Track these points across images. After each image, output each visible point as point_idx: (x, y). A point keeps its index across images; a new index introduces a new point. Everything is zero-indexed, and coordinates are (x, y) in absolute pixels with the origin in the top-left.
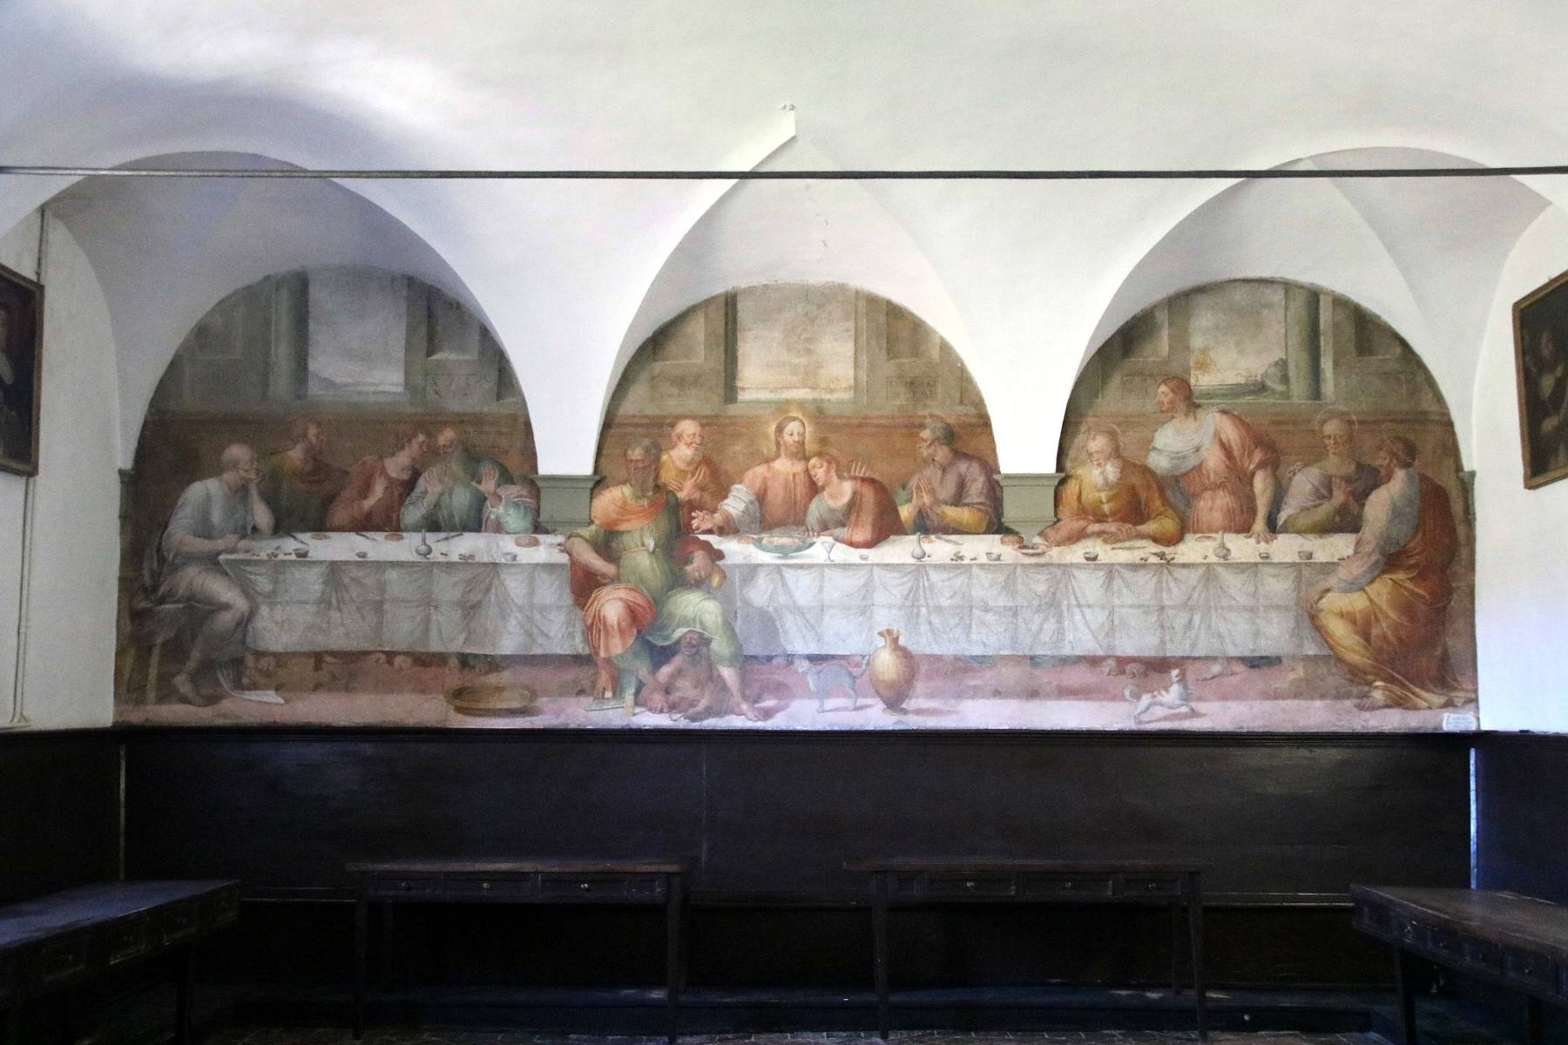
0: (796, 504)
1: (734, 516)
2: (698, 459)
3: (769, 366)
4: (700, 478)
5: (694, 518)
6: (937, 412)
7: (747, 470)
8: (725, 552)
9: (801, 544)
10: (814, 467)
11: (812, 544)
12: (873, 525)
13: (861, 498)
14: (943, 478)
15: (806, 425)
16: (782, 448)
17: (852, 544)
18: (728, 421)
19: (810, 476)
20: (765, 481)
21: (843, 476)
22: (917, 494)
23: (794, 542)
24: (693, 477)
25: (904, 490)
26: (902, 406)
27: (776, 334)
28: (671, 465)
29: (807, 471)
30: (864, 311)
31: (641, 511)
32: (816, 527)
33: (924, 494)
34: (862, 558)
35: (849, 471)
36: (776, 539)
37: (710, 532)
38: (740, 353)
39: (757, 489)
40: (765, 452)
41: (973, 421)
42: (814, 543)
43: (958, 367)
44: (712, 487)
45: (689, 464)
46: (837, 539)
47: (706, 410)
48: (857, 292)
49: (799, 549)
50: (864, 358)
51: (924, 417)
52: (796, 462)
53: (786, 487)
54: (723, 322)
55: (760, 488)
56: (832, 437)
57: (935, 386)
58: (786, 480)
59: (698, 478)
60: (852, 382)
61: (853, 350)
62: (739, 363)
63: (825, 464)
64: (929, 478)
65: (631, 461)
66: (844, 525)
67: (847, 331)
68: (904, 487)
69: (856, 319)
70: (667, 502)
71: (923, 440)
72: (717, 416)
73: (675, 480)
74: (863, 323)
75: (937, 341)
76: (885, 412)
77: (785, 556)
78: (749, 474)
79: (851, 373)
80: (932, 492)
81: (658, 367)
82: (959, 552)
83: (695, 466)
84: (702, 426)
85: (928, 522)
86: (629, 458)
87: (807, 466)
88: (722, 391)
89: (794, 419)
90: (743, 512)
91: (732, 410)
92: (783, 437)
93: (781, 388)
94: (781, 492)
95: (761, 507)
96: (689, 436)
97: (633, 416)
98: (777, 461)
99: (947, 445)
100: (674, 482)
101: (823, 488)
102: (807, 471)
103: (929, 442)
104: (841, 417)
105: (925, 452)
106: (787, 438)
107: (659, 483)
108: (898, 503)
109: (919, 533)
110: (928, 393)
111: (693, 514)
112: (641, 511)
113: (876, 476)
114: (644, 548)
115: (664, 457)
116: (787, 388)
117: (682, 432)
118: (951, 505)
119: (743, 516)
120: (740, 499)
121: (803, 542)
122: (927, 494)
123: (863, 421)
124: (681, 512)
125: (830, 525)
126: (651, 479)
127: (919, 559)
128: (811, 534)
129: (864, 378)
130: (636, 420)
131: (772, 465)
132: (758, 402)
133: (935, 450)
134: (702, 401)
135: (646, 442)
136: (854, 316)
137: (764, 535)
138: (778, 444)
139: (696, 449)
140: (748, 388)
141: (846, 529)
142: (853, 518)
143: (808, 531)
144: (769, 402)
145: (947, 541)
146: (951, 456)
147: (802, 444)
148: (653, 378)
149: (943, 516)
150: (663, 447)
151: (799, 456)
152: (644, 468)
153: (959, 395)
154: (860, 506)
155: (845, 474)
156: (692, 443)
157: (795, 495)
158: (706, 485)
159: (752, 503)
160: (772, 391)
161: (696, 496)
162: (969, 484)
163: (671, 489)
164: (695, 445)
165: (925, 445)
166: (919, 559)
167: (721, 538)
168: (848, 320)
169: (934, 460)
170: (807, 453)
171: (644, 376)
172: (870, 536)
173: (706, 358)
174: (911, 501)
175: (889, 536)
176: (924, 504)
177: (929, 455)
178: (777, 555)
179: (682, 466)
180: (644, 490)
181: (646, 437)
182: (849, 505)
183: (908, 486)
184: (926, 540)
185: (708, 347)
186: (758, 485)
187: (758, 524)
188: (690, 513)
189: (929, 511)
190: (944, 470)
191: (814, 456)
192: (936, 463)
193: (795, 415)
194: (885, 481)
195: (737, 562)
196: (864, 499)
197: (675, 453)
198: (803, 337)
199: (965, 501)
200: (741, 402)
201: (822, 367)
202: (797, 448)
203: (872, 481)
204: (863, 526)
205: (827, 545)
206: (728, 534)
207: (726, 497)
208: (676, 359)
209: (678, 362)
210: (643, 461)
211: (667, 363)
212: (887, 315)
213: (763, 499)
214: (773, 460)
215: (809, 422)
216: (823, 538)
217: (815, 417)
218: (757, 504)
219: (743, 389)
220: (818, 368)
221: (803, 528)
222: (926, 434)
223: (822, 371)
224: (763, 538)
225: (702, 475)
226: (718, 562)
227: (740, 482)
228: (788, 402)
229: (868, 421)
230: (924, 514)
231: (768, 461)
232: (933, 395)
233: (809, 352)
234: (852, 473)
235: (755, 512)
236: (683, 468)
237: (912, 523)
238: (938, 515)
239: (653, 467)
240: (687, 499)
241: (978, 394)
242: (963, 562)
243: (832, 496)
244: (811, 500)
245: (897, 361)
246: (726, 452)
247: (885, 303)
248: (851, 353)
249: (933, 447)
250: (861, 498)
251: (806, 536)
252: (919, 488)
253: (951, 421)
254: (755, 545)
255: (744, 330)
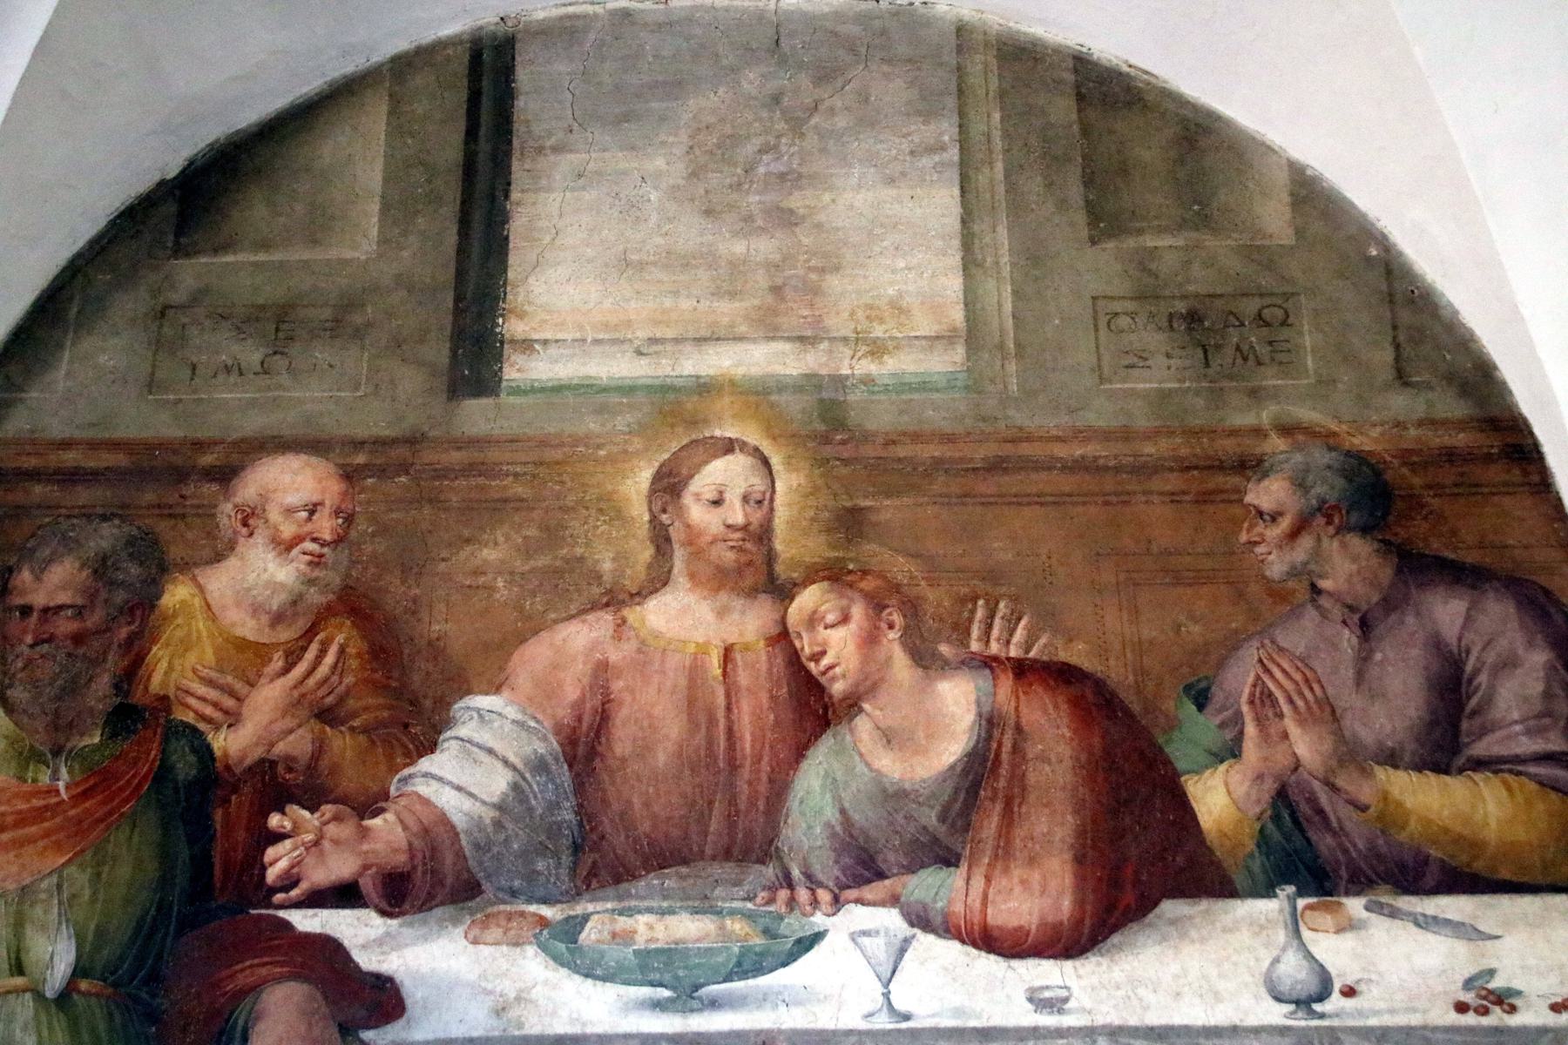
0: (733, 766)
1: (459, 820)
2: (316, 598)
3: (627, 265)
4: (324, 670)
5: (278, 837)
6: (1307, 414)
7: (522, 639)
8: (413, 993)
9: (758, 941)
10: (813, 620)
11: (807, 943)
12: (1079, 860)
13: (1016, 749)
14: (1363, 660)
15: (776, 461)
16: (679, 557)
17: (990, 940)
18: (456, 457)
19: (794, 661)
20: (602, 669)
21: (935, 655)
22: (1260, 721)
23: (724, 933)
24: (286, 670)
25: (1201, 707)
26: (1164, 396)
27: (660, 163)
28: (201, 625)
29: (782, 637)
30: (994, 83)
31: (38, 815)
32: (826, 867)
33: (1294, 731)
34: (1040, 1000)
35: (961, 632)
36: (642, 920)
37: (344, 895)
38: (517, 227)
39: (564, 714)
40: (607, 566)
41: (1461, 439)
42: (817, 937)
43: (1369, 260)
44: (369, 709)
45: (278, 619)
46: (921, 920)
47: (375, 421)
48: (962, 30)
49: (752, 964)
50: (1000, 239)
51: (1258, 432)
52: (738, 603)
53: (691, 702)
54: (462, 125)
55: (578, 705)
56: (888, 511)
57: (1284, 323)
58: (695, 672)
59: (310, 672)
60: (957, 315)
61: (956, 210)
62: (513, 259)
63: (858, 611)
64: (1304, 661)
65: (26, 610)
66: (949, 860)
67: (931, 150)
68: (1201, 700)
69: (962, 114)
70: (163, 773)
71: (1260, 514)
72: (413, 441)
73: (210, 683)
74: (990, 121)
75: (1282, 177)
76: (1100, 415)
77: (687, 996)
78: (534, 656)
79: (953, 285)
80: (1327, 713)
81: (189, 274)
82: (1491, 973)
83: (302, 624)
84: (350, 475)
85: (1325, 843)
86: (19, 601)
87: (783, 621)
88: (438, 351)
89: (729, 447)
90: (500, 807)
91: (475, 416)
92: (681, 511)
93: (676, 341)
94: (673, 728)
95: (579, 787)
96: (290, 511)
97: (66, 444)
98: (652, 604)
99: (1365, 530)
100: (202, 690)
101: (853, 704)
102: (782, 637)
103: (1285, 523)
104: (916, 437)
105: (1276, 567)
106: (697, 513)
107: (138, 698)
108: (1180, 765)
109: (1291, 889)
110: (1263, 351)
111: (275, 820)
112: (38, 815)
113: (1077, 654)
114: (19, 981)
115: (177, 594)
116: (700, 341)
117: (264, 497)
118: (1419, 768)
119: (498, 824)
120: (490, 751)
121: (767, 932)
122: (1301, 722)
123: (1008, 449)
124: (218, 815)
125: (890, 858)
126: (102, 685)
127: (1304, 1003)
128: (803, 894)
129: (1000, 297)
130: (70, 458)
131: (632, 614)
132: (585, 389)
133: (1317, 553)
134: (357, 389)
135: (105, 537)
136: (951, 102)
137: (590, 907)
138: (661, 540)
139: (317, 561)
140: (545, 342)
141: (956, 877)
142: (989, 825)
143: (790, 884)
144: (628, 389)
145: (1427, 923)
146: (1386, 574)
147: (762, 535)
148: (162, 313)
149: (1389, 817)
150: (175, 552)
151: (749, 581)
152: (78, 639)
153: (1388, 355)
154: (1018, 776)
155: (944, 649)
156: (298, 540)
157: (730, 732)
158: (341, 700)
159: (540, 766)
160: (639, 353)
161: (297, 744)
162: (1483, 678)
163: (190, 718)
164: (309, 546)
165: (1275, 532)
166: (1304, 1003)
167: (394, 923)
168: (928, 115)
169: (1315, 590)
170: (779, 568)
171: (129, 304)
172: (1067, 904)
173: (383, 241)
174: (1233, 751)
175: (1156, 904)
176: (1297, 766)
177: (1294, 572)
178: (645, 992)
179: (248, 628)
180: (61, 727)
181: (104, 518)
182: (965, 772)
183: (1218, 696)
184: (1327, 920)
185: (397, 209)
186: (572, 693)
187: (566, 859)
188: (266, 816)
189: (1316, 785)
190: (1365, 627)
191: (808, 581)
192: (1324, 602)
193: (731, 433)
194: (1117, 673)
195: (457, 1031)
196: (1033, 749)
197: (220, 581)
198: (762, 170)
199: (1480, 749)
200: (517, 391)
201: (837, 269)
202: (741, 550)
203: (1061, 675)
204: (1032, 861)
205: (877, 946)
206: (426, 905)
207: (430, 747)
208: (265, 245)
209: (277, 256)
210: (79, 611)
211: (230, 258)
212: (1080, 98)
213: (592, 753)
214: (640, 595)
215: (788, 460)
216: (857, 916)
217: (814, 436)
218: (565, 776)
219: (527, 345)
220: (822, 271)
221: (770, 872)
222: (1269, 493)
223: (834, 282)
224: (586, 918)
225: (330, 659)
226: (367, 1035)
227: (497, 690)
228: (705, 388)
229: (1026, 449)
230: (1304, 808)
231: (616, 599)
232: (1282, 355)
233: (786, 219)
234: (975, 646)
235: (553, 806)
236: (251, 636)
237: (1251, 845)
238: (1363, 808)
239: (124, 632)
240: (258, 753)
241: (1464, 342)
242: (1515, 1021)
243: (889, 737)
244: (800, 752)
245: (1131, 243)
246: (442, 566)
247: (1070, 63)
248: (953, 221)
249: (1306, 542)
250: (1016, 749)
251: (779, 906)
252: (1263, 699)
253: (1363, 442)
254: (544, 948)
255: (540, 150)
